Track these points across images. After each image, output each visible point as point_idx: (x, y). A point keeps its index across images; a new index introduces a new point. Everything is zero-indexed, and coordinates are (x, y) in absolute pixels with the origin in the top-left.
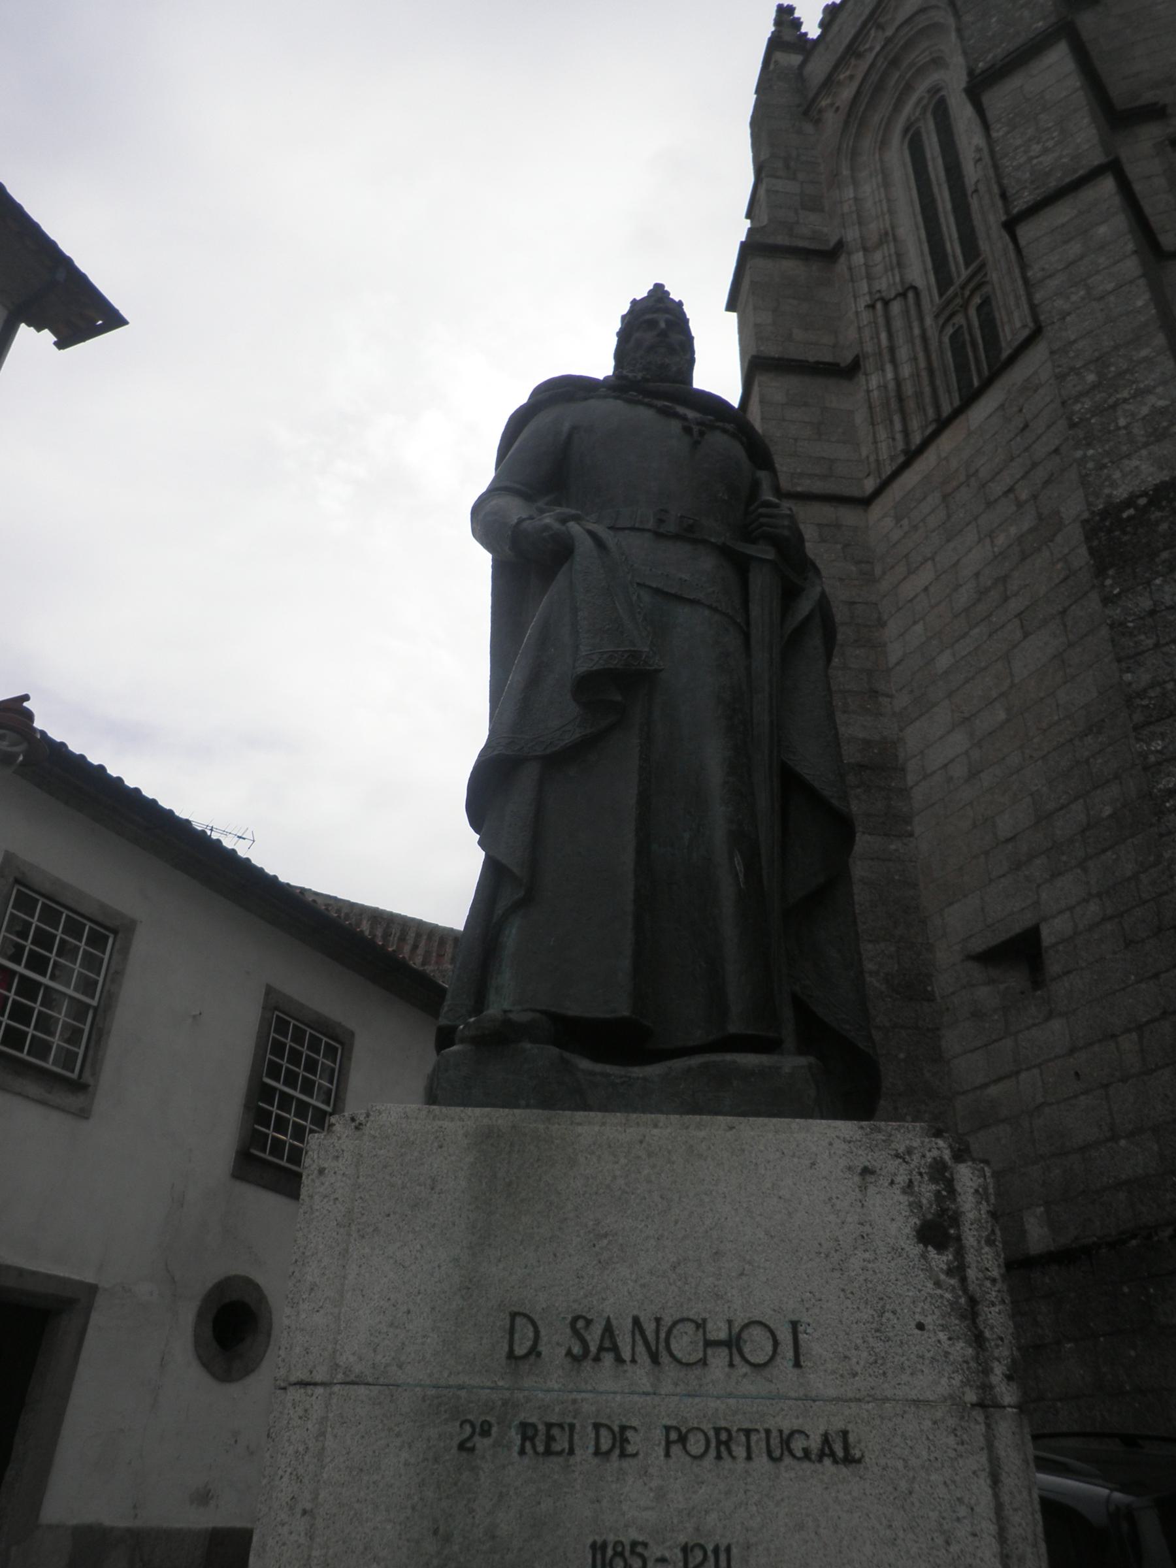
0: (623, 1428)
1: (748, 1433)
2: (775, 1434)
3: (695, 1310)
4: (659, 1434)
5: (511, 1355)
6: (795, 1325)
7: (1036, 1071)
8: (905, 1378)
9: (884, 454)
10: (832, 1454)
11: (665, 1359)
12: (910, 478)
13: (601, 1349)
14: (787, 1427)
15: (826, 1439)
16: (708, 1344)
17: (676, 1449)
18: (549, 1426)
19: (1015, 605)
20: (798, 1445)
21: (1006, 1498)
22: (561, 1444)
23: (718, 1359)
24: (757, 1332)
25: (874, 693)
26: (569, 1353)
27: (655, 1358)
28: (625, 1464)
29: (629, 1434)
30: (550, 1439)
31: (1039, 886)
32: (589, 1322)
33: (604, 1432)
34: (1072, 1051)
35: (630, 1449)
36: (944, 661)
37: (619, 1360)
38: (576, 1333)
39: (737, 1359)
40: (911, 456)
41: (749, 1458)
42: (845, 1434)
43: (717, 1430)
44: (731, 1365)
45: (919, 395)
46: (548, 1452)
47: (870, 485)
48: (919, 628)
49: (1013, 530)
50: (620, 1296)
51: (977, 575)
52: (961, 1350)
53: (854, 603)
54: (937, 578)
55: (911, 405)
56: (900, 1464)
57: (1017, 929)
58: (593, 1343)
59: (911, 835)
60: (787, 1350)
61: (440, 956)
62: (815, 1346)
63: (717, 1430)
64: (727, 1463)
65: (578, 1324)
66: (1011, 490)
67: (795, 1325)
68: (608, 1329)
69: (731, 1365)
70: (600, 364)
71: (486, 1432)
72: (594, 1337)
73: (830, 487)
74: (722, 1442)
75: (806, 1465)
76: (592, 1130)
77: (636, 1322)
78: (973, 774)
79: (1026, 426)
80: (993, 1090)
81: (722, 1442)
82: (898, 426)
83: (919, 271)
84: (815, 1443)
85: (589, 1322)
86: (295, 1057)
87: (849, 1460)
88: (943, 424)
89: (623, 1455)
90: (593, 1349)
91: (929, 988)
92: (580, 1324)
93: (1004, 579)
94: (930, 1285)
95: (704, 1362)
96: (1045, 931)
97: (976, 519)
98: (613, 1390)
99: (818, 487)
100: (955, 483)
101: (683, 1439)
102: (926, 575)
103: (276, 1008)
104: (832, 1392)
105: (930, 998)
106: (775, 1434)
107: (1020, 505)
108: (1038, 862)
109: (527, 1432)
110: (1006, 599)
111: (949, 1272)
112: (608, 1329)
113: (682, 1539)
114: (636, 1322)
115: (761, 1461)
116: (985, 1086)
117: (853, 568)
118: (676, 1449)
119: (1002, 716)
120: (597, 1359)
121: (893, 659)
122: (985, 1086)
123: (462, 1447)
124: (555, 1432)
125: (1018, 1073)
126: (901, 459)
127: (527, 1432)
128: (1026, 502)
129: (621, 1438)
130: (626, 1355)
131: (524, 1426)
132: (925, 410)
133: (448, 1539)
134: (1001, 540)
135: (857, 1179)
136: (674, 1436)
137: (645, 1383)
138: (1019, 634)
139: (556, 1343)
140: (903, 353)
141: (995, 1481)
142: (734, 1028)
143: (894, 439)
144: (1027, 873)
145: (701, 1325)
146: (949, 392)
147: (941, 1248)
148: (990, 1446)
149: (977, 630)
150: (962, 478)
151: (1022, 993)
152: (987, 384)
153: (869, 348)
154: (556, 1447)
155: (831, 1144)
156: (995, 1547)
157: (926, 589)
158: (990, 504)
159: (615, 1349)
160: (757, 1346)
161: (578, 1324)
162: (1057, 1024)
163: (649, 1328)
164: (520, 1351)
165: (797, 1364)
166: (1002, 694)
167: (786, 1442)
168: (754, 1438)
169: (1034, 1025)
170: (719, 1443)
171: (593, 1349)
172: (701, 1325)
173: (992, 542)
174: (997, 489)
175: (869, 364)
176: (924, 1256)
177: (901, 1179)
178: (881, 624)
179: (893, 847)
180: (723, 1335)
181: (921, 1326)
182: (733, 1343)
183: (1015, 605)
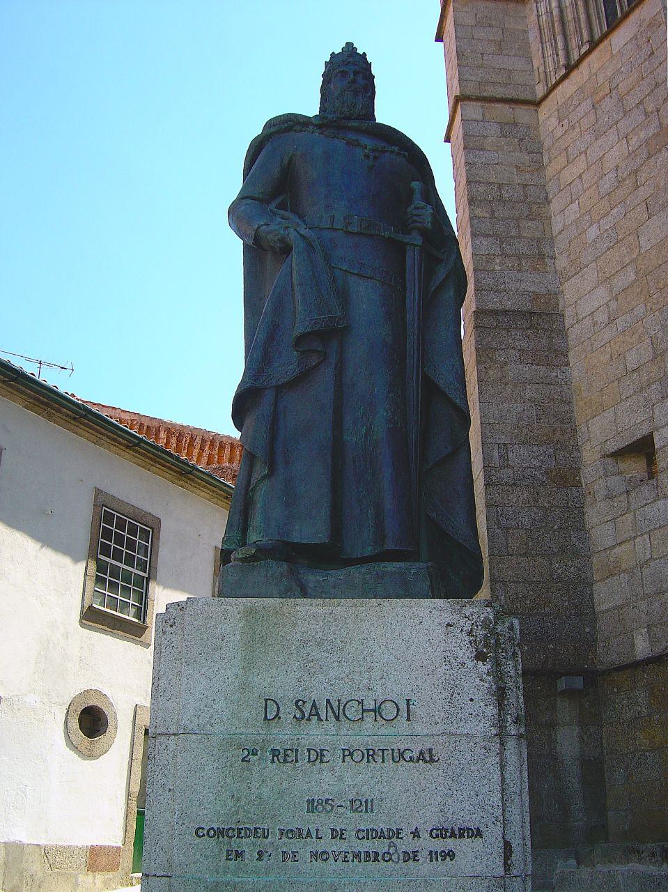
0: (322, 750)
1: (383, 750)
2: (396, 751)
3: (358, 696)
4: (339, 753)
5: (266, 718)
7: (646, 536)
8: (462, 724)
9: (551, 68)
10: (424, 759)
11: (342, 718)
12: (568, 88)
13: (310, 714)
15: (421, 753)
17: (348, 759)
18: (286, 750)
19: (643, 193)
20: (407, 755)
21: (507, 776)
22: (292, 757)
24: (388, 704)
25: (542, 256)
26: (295, 717)
28: (323, 766)
29: (325, 752)
31: (654, 405)
32: (304, 702)
33: (312, 752)
35: (325, 759)
36: (592, 233)
37: (320, 719)
39: (379, 718)
40: (570, 68)
41: (383, 762)
43: (368, 750)
44: (376, 720)
45: (577, 19)
46: (285, 761)
47: (540, 90)
48: (575, 206)
49: (642, 135)
50: (320, 692)
51: (617, 168)
52: (491, 711)
53: (527, 185)
54: (588, 168)
55: (571, 28)
56: (457, 762)
57: (638, 435)
58: (307, 712)
59: (568, 364)
61: (220, 457)
62: (417, 711)
63: (368, 750)
64: (373, 764)
66: (641, 102)
67: (408, 701)
68: (314, 705)
69: (376, 720)
70: (310, 106)
71: (255, 754)
72: (307, 709)
73: (511, 93)
74: (370, 755)
75: (411, 764)
76: (305, 608)
77: (328, 701)
78: (611, 320)
79: (653, 53)
80: (617, 550)
81: (370, 755)
82: (560, 45)
84: (415, 755)
85: (304, 702)
86: (119, 539)
87: (432, 761)
88: (594, 45)
89: (322, 762)
90: (307, 715)
91: (577, 478)
92: (300, 703)
93: (636, 172)
94: (478, 680)
95: (362, 719)
96: (656, 437)
97: (616, 123)
98: (316, 734)
99: (499, 92)
100: (601, 94)
101: (351, 754)
102: (580, 165)
103: (103, 505)
104: (425, 732)
105: (578, 484)
106: (396, 751)
107: (647, 115)
108: (654, 387)
109: (275, 753)
110: (638, 187)
111: (488, 674)
112: (314, 705)
113: (350, 797)
114: (328, 701)
115: (390, 763)
117: (527, 158)
118: (348, 759)
119: (632, 277)
120: (309, 719)
121: (556, 228)
122: (613, 547)
123: (243, 760)
124: (289, 752)
125: (635, 538)
126: (563, 72)
127: (275, 753)
128: (652, 113)
129: (320, 755)
130: (323, 717)
131: (273, 750)
132: (581, 33)
133: (238, 799)
134: (634, 141)
135: (444, 629)
136: (347, 753)
137: (333, 730)
138: (645, 216)
139: (288, 712)
141: (502, 767)
142: (390, 545)
143: (557, 55)
144: (646, 395)
145: (361, 702)
146: (599, 18)
147: (484, 660)
148: (501, 753)
149: (615, 210)
150: (607, 91)
151: (641, 481)
152: (626, 16)
154: (289, 759)
155: (431, 612)
156: (500, 796)
158: (626, 113)
159: (318, 714)
163: (335, 705)
164: (270, 717)
165: (408, 719)
166: (634, 260)
167: (401, 755)
168: (386, 752)
169: (646, 504)
170: (369, 755)
171: (307, 715)
172: (361, 702)
173: (628, 143)
174: (631, 102)
176: (475, 666)
177: (467, 628)
178: (548, 201)
179: (554, 374)
180: (372, 707)
181: (471, 700)
182: (377, 711)
183: (643, 193)
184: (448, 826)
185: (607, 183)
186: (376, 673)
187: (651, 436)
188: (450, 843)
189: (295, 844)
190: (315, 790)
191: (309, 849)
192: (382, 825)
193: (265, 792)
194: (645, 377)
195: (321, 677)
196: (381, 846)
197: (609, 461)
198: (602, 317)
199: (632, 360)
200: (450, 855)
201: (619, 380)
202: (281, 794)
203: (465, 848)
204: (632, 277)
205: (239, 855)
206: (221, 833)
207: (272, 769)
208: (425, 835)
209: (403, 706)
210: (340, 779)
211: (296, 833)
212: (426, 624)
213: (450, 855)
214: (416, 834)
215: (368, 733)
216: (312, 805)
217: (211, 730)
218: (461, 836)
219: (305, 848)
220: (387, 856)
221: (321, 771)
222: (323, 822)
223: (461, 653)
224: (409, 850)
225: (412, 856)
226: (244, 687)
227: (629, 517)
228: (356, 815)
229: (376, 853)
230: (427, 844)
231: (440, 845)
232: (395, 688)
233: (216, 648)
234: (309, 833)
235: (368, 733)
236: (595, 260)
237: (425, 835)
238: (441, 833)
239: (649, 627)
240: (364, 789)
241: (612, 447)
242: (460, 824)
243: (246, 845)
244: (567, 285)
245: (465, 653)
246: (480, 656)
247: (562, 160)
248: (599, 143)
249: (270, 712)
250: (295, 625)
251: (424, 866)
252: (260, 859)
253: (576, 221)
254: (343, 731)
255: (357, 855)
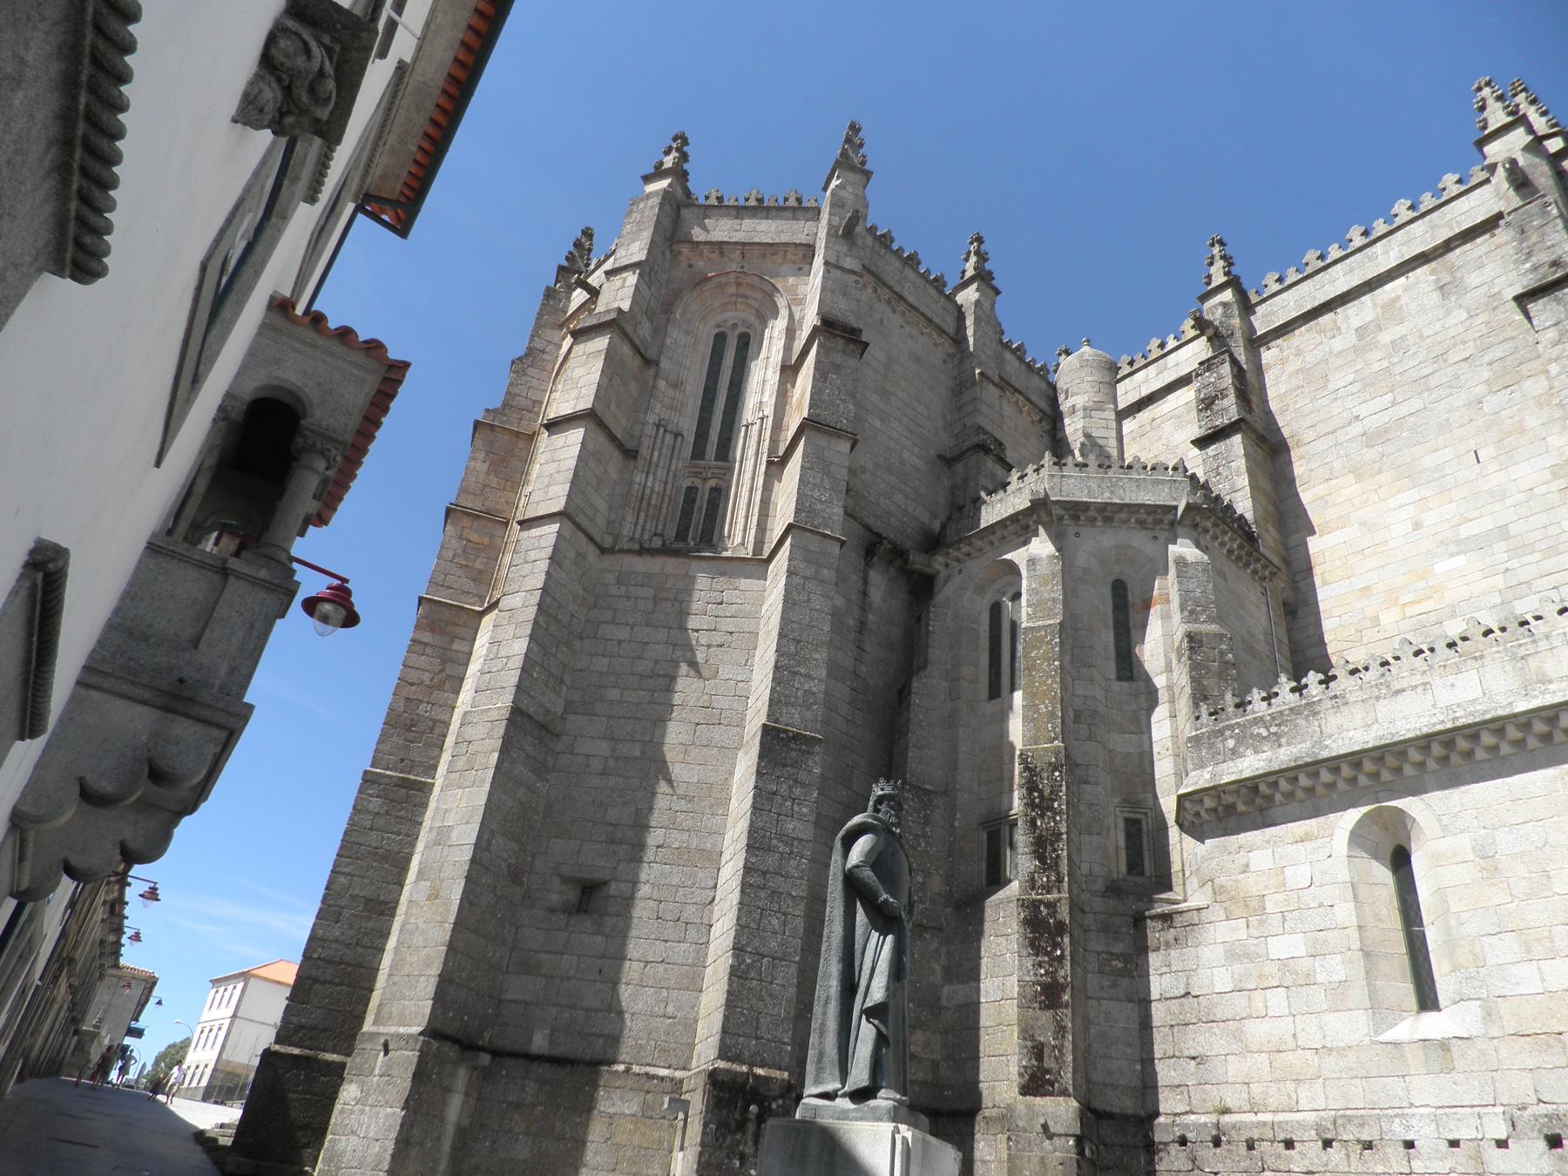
34: (603, 957)
36: (613, 694)
48: (606, 660)
51: (656, 661)
55: (651, 511)
57: (597, 875)
78: (604, 773)
80: (542, 956)
82: (641, 521)
83: (688, 425)
96: (613, 886)
102: (623, 633)
116: (538, 952)
119: (637, 753)
122: (538, 952)
140: (661, 473)
153: (644, 451)
157: (620, 642)
162: (599, 939)
175: (640, 463)
185: (643, 666)
187: (606, 883)
194: (620, 835)
197: (556, 880)
198: (596, 765)
199: (613, 814)
201: (595, 823)
204: (637, 753)
227: (565, 935)
236: (609, 717)
239: (553, 1031)
241: (567, 871)
244: (572, 717)
247: (608, 615)
248: (648, 630)
253: (602, 673)
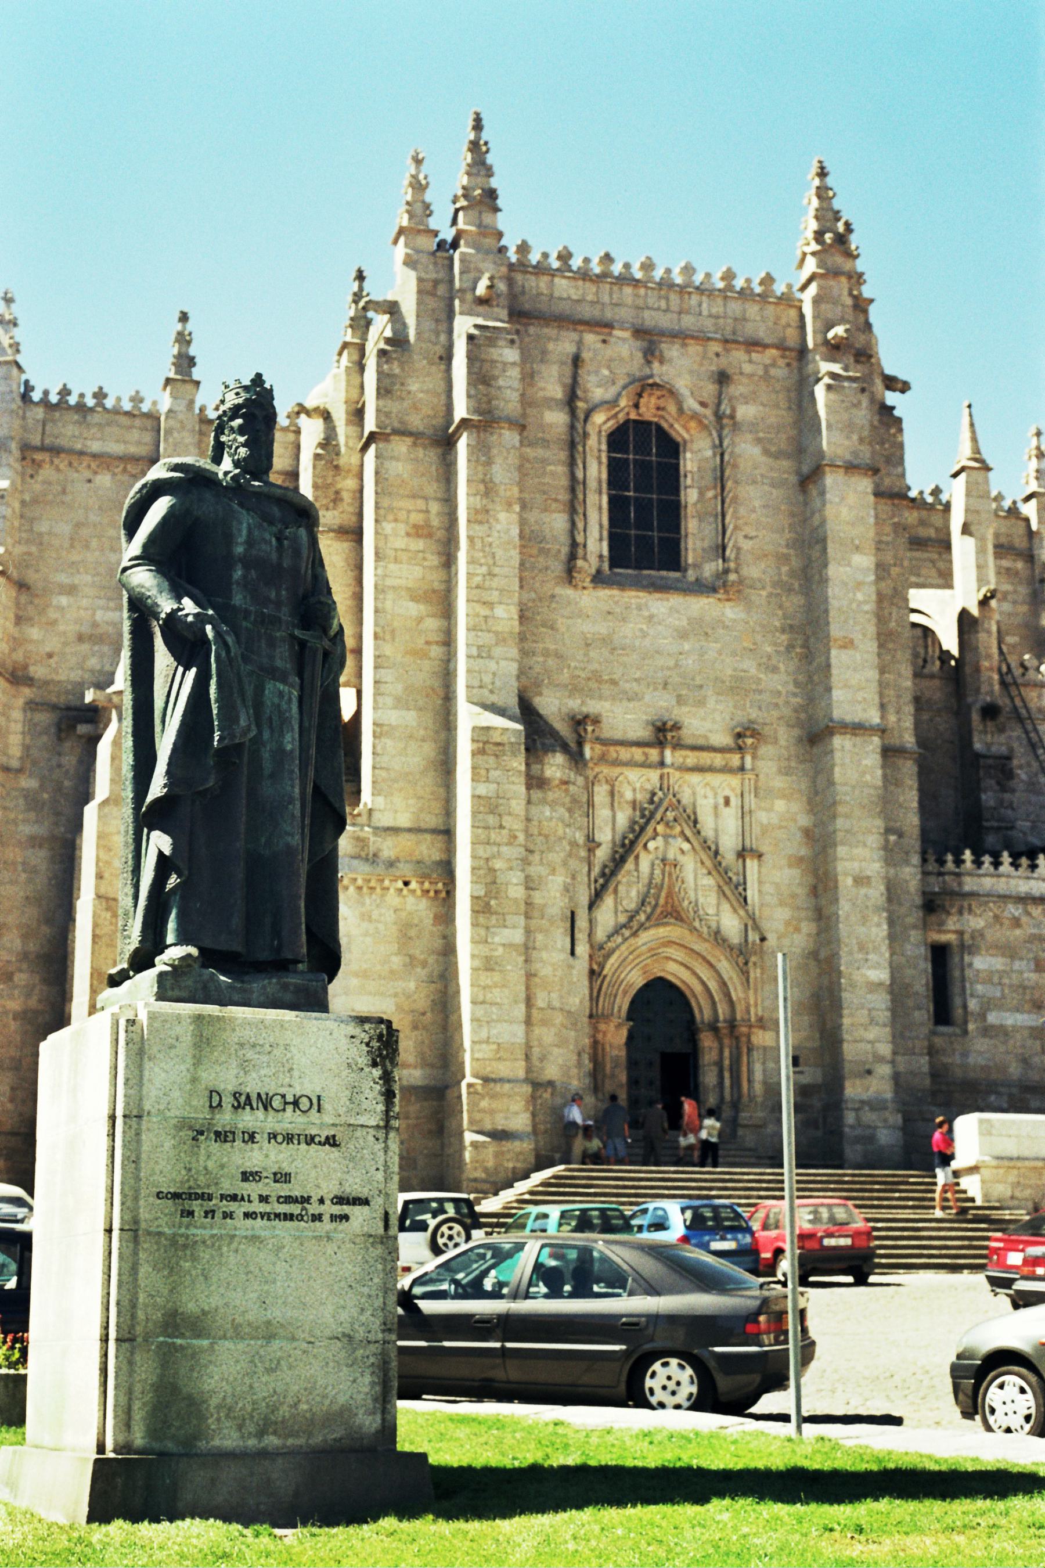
3: (282, 1091)
4: (266, 1136)
5: (211, 1106)
6: (319, 1097)
14: (313, 1133)
15: (327, 1138)
16: (286, 1103)
20: (317, 1139)
22: (230, 1137)
23: (290, 1108)
24: (304, 1100)
27: (266, 1109)
30: (226, 1136)
37: (252, 1108)
38: (236, 1098)
42: (334, 1136)
46: (226, 1141)
50: (253, 1086)
58: (243, 1102)
60: (315, 1107)
62: (326, 1105)
65: (236, 1095)
67: (319, 1097)
72: (243, 1099)
74: (289, 1138)
77: (259, 1095)
81: (289, 1138)
84: (323, 1140)
95: (284, 1110)
98: (249, 1119)
101: (275, 1137)
109: (218, 1134)
112: (248, 1097)
114: (259, 1095)
115: (303, 1146)
123: (193, 1139)
129: (252, 1137)
133: (190, 1170)
139: (228, 1101)
145: (283, 1096)
160: (304, 1104)
161: (236, 1095)
163: (264, 1097)
165: (319, 1111)
172: (283, 1096)
177: (366, 1040)
182: (296, 1103)
184: (344, 1195)
186: (296, 1073)
188: (346, 1209)
189: (233, 1206)
190: (248, 1164)
191: (243, 1210)
192: (296, 1193)
193: (210, 1164)
195: (254, 1075)
196: (296, 1209)
200: (345, 1217)
202: (222, 1166)
203: (357, 1213)
205: (191, 1213)
206: (176, 1196)
207: (215, 1147)
208: (328, 1202)
209: (315, 1101)
210: (267, 1156)
211: (234, 1198)
212: (335, 1035)
213: (345, 1217)
214: (322, 1201)
215: (290, 1121)
216: (246, 1176)
217: (168, 1114)
218: (354, 1204)
219: (239, 1209)
220: (300, 1218)
221: (252, 1150)
222: (252, 1189)
223: (360, 1060)
224: (317, 1212)
225: (317, 1218)
226: (194, 1080)
228: (278, 1185)
229: (292, 1215)
230: (330, 1209)
231: (337, 1210)
232: (306, 1086)
233: (172, 1047)
234: (243, 1199)
235: (290, 1121)
237: (328, 1202)
238: (340, 1200)
240: (284, 1165)
242: (354, 1194)
243: (196, 1206)
245: (363, 1061)
246: (374, 1064)
249: (214, 1100)
250: (234, 1030)
251: (327, 1225)
252: (206, 1217)
254: (270, 1119)
255: (277, 1216)
